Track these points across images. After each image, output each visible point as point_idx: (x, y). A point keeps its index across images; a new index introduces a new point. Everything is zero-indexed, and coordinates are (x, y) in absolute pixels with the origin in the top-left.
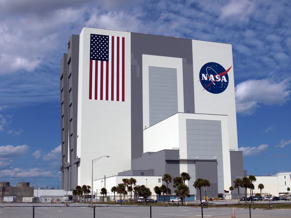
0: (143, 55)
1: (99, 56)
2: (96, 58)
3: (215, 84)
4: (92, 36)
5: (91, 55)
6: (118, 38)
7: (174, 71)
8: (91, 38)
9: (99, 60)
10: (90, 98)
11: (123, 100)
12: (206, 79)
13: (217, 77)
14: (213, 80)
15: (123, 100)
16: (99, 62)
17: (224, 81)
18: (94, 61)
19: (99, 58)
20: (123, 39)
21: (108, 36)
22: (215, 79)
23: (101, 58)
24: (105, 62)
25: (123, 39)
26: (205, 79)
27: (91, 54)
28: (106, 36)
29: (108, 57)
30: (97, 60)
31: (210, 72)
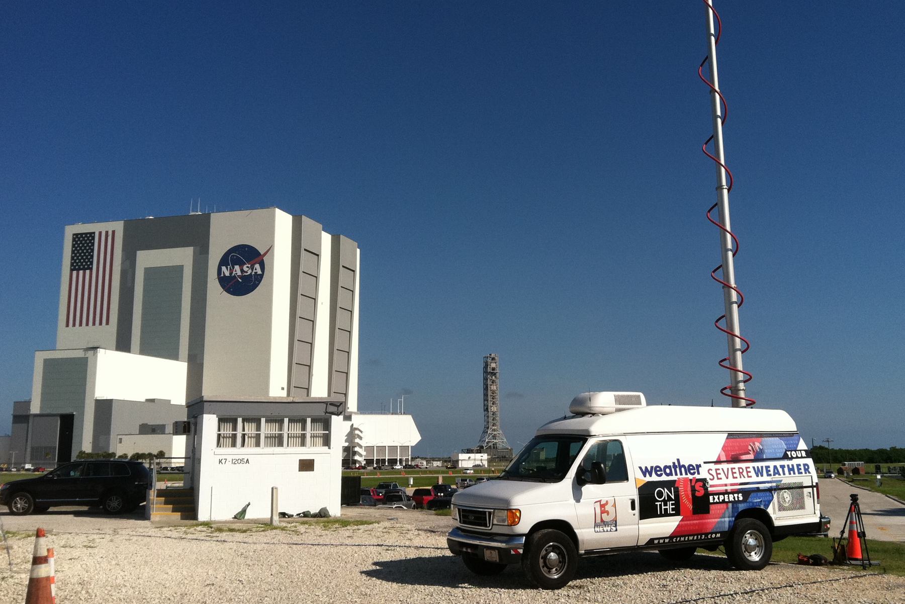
5: (72, 264)
7: (179, 269)
8: (74, 240)
10: (67, 325)
11: (107, 323)
12: (227, 274)
13: (245, 268)
14: (239, 273)
15: (107, 323)
20: (114, 232)
25: (114, 232)
29: (92, 263)
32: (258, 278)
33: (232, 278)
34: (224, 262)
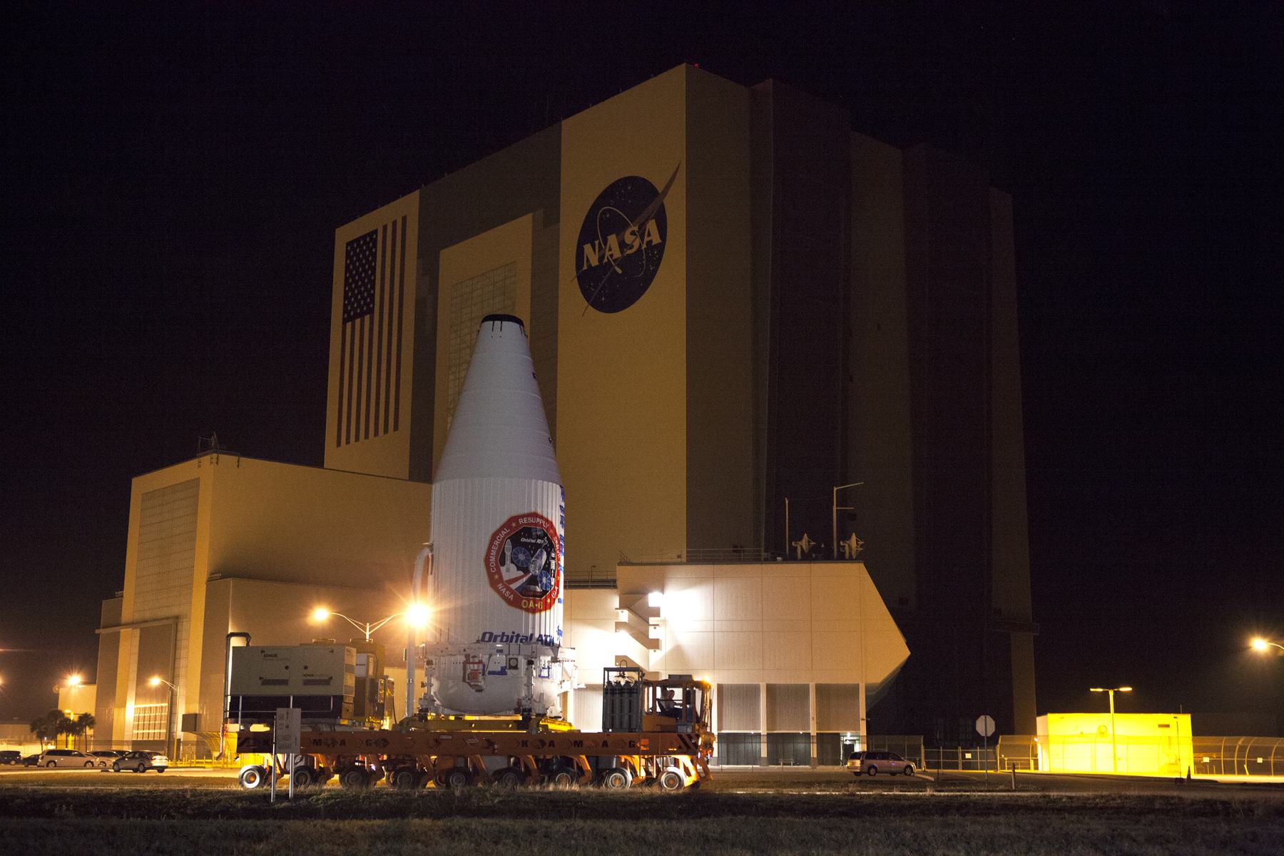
1: (359, 306)
3: (620, 271)
8: (348, 256)
12: (595, 262)
13: (628, 238)
14: (617, 254)
17: (650, 242)
18: (349, 325)
20: (404, 219)
21: (375, 232)
22: (622, 252)
23: (361, 308)
24: (367, 317)
25: (404, 219)
26: (589, 266)
30: (356, 316)
32: (655, 255)
33: (604, 267)
34: (588, 234)
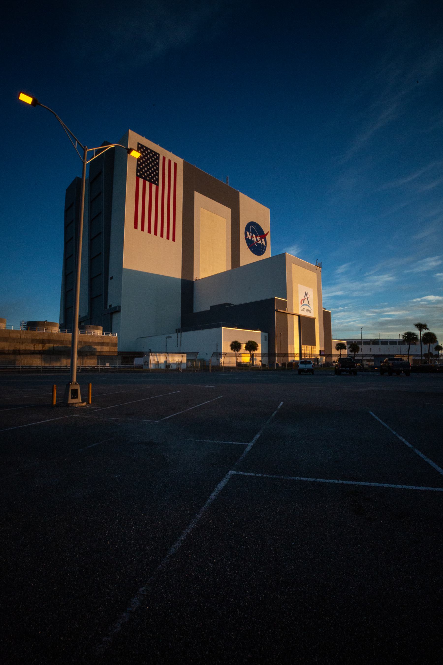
0: (195, 192)
2: (143, 176)
4: (140, 146)
5: (138, 171)
6: (170, 161)
9: (148, 181)
10: (136, 227)
11: (174, 240)
12: (250, 238)
14: (255, 241)
15: (174, 240)
16: (148, 184)
18: (141, 181)
19: (148, 178)
20: (175, 164)
21: (159, 155)
24: (154, 186)
25: (175, 164)
27: (137, 169)
28: (156, 153)
29: (157, 180)
31: (253, 232)
